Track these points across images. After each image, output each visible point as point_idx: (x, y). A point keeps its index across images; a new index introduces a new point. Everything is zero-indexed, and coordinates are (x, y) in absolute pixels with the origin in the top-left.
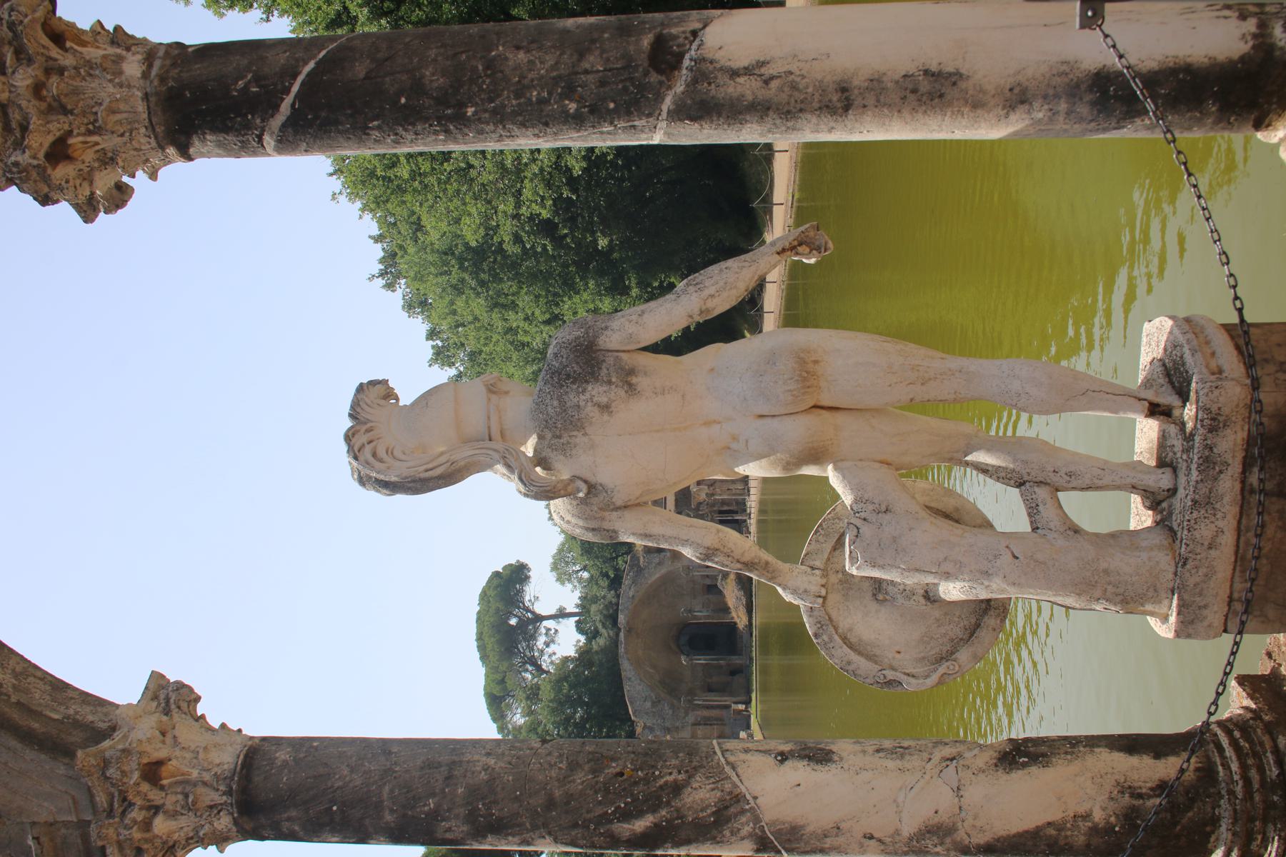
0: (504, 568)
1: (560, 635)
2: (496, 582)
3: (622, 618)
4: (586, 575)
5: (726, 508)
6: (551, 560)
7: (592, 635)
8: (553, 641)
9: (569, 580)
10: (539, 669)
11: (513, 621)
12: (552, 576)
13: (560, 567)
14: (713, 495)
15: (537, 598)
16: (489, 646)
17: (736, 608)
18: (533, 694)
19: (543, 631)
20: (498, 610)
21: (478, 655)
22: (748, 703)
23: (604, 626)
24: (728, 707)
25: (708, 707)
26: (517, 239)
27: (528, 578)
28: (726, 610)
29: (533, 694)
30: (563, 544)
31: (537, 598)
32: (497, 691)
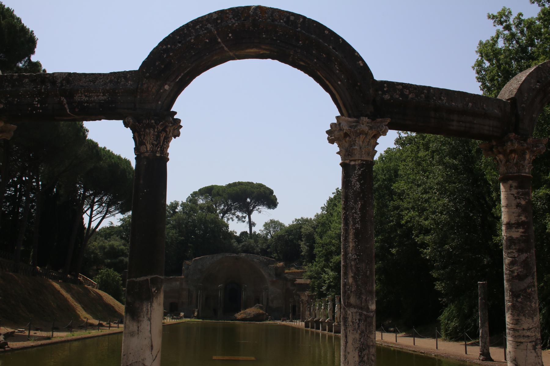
0: (275, 196)
1: (242, 223)
2: (268, 192)
3: (244, 255)
4: (269, 237)
5: (297, 309)
6: (276, 220)
7: (239, 239)
8: (239, 220)
9: (266, 229)
10: (224, 212)
11: (248, 200)
12: (268, 220)
13: (272, 224)
14: (302, 303)
15: (260, 212)
16: (235, 188)
17: (245, 313)
18: (210, 210)
19: (244, 215)
20: (253, 192)
21: (231, 182)
22: (198, 317)
23: (243, 246)
24: (197, 306)
25: (197, 297)
26: (397, 208)
27: (269, 207)
28: (245, 308)
29: (210, 210)
30: (284, 226)
31: (260, 212)
32: (214, 191)
